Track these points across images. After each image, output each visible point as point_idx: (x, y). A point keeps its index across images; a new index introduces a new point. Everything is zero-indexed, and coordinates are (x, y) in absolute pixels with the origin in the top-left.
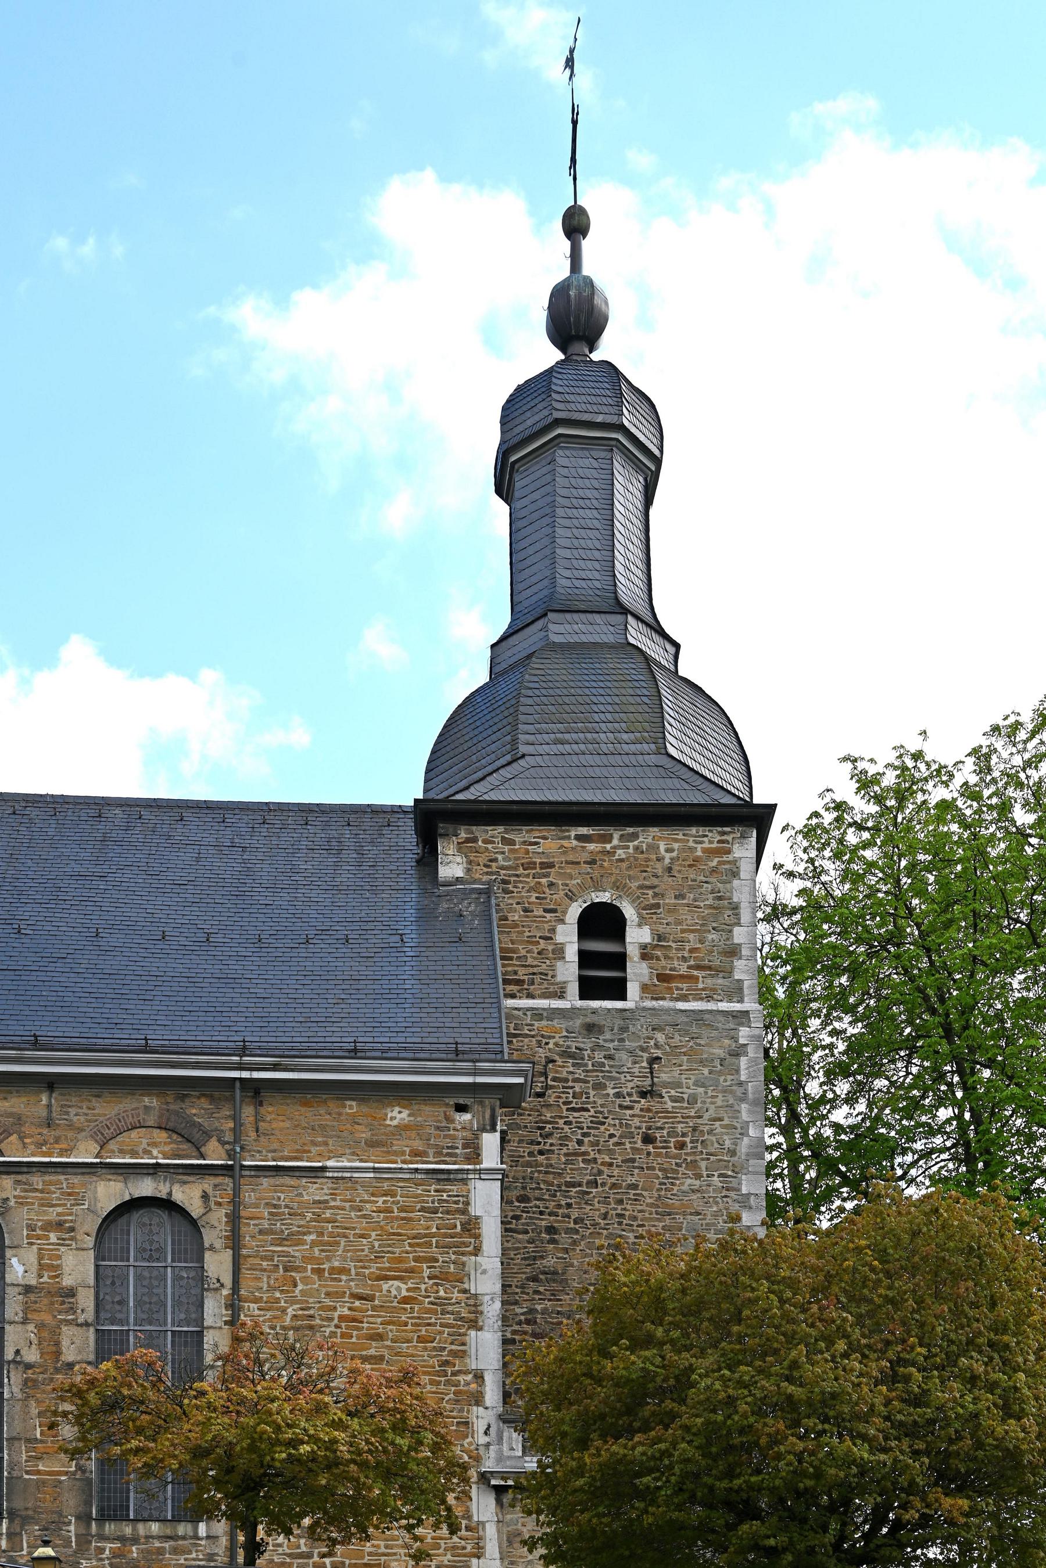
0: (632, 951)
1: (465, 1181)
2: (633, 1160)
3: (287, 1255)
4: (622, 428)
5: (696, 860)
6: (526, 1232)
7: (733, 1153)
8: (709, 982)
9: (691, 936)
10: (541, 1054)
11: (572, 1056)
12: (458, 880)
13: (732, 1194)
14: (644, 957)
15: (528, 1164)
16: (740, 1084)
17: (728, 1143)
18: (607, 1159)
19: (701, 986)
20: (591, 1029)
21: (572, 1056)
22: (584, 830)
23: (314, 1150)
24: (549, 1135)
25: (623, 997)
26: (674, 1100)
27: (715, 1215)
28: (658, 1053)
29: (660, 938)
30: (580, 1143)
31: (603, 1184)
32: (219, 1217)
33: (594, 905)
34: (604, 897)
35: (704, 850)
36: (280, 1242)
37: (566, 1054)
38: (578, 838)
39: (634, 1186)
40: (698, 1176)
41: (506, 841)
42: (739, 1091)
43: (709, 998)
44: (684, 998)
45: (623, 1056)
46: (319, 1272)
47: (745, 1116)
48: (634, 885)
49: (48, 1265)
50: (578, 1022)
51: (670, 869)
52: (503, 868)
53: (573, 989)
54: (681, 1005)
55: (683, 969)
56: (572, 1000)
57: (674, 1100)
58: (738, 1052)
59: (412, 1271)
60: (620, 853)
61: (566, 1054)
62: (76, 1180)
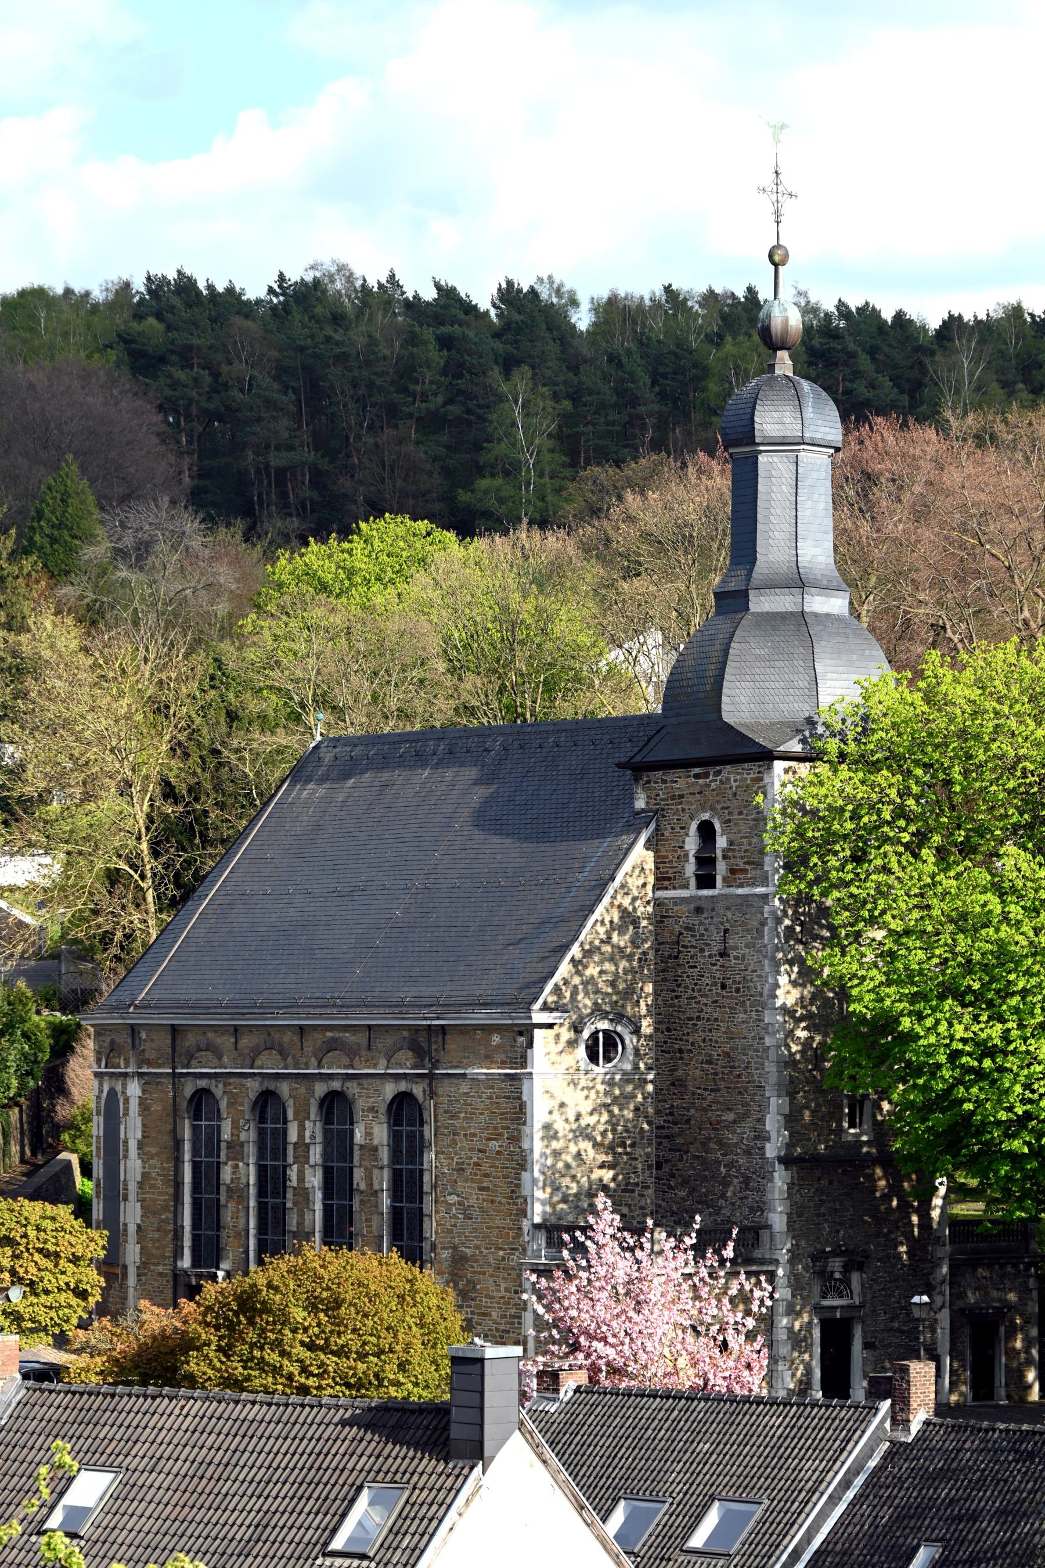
0: (719, 854)
1: (520, 1080)
3: (453, 1125)
5: (748, 786)
9: (745, 841)
10: (677, 928)
14: (725, 857)
20: (699, 910)
22: (697, 770)
23: (465, 1061)
24: (679, 986)
25: (714, 887)
28: (728, 925)
34: (706, 816)
37: (687, 929)
39: (716, 1020)
40: (745, 1012)
44: (741, 886)
45: (712, 928)
46: (465, 1135)
49: (369, 1134)
50: (692, 906)
53: (693, 882)
54: (740, 891)
55: (742, 866)
56: (692, 891)
57: (736, 958)
58: (763, 924)
59: (500, 1135)
61: (687, 929)
62: (378, 1082)
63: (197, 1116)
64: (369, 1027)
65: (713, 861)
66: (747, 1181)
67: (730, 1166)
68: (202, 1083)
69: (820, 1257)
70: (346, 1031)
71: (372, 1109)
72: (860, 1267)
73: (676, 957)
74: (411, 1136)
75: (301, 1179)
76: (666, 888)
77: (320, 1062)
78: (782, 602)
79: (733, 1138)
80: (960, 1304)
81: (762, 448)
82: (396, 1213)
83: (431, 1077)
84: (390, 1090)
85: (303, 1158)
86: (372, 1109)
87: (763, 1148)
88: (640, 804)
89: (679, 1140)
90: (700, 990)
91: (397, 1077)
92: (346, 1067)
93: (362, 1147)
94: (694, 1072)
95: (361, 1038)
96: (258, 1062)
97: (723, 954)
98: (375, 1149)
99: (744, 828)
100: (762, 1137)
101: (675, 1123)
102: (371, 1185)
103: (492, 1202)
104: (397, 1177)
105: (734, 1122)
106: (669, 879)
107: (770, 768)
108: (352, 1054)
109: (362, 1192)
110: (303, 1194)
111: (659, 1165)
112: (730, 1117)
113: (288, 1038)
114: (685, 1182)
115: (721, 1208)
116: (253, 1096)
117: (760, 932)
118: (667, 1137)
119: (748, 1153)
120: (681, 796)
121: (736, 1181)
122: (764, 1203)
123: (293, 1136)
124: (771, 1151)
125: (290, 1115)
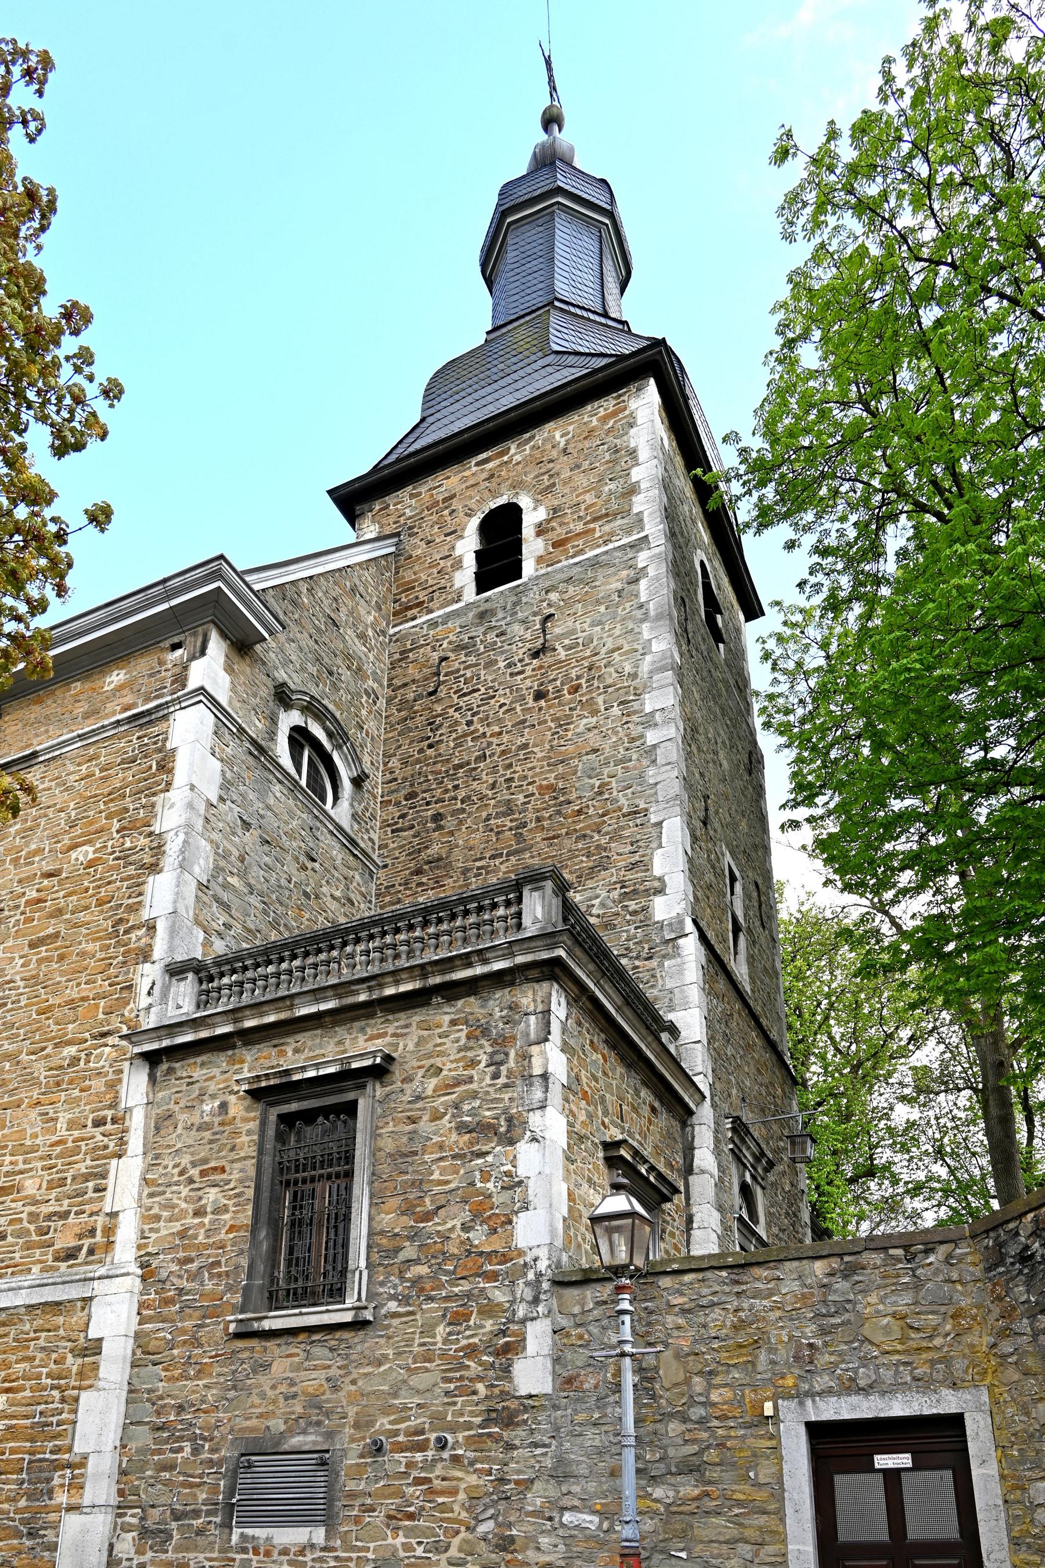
2: (524, 721)
4: (560, 191)
6: (412, 827)
7: (634, 676)
8: (607, 528)
10: (436, 656)
11: (463, 647)
13: (635, 718)
15: (418, 761)
17: (628, 668)
18: (497, 729)
19: (597, 535)
21: (463, 647)
27: (615, 747)
29: (555, 510)
30: (469, 723)
31: (492, 755)
33: (492, 511)
35: (599, 420)
37: (460, 647)
38: (477, 464)
39: (525, 746)
40: (595, 712)
42: (639, 614)
43: (605, 543)
48: (529, 478)
51: (565, 450)
52: (410, 518)
55: (579, 527)
57: (568, 648)
60: (518, 458)
61: (460, 647)
73: (431, 694)
76: (414, 618)
90: (481, 720)
106: (420, 604)
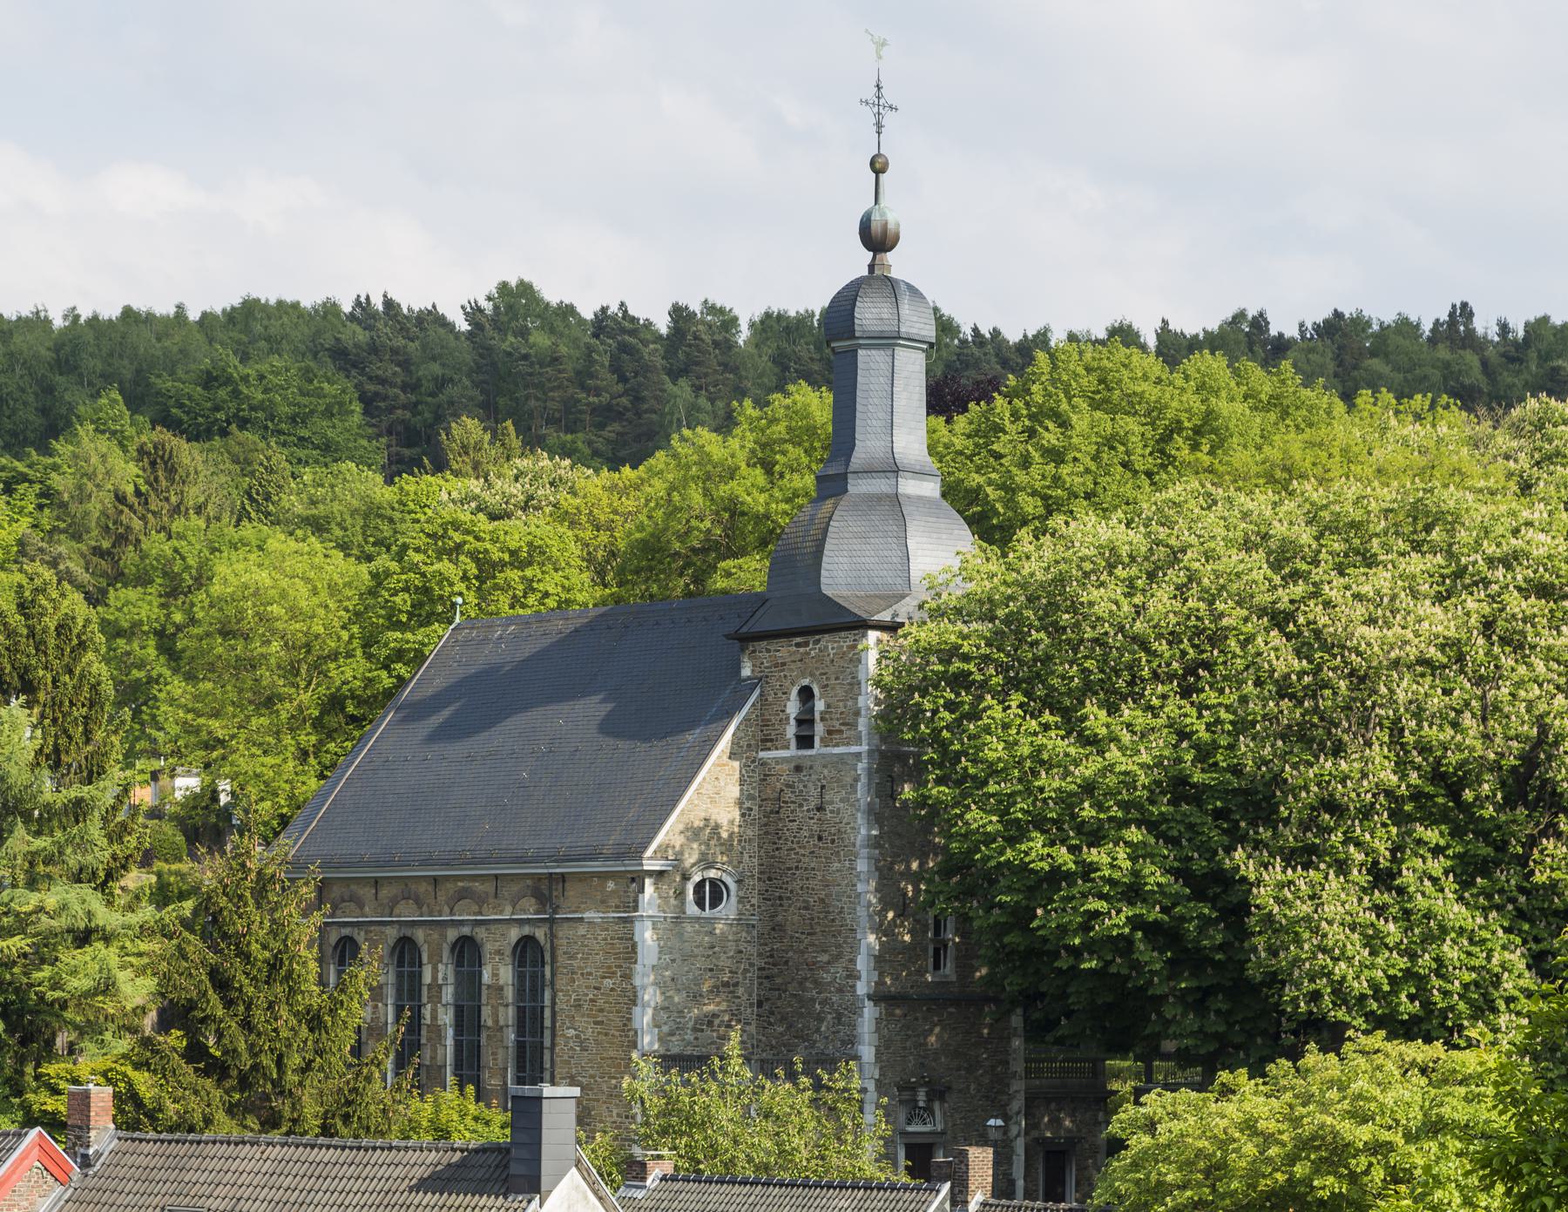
0: (817, 716)
1: (632, 922)
3: (571, 965)
5: (844, 653)
7: (854, 845)
9: (841, 704)
12: (749, 678)
14: (822, 719)
16: (858, 800)
22: (798, 640)
24: (779, 839)
26: (832, 812)
28: (824, 782)
32: (548, 945)
34: (806, 682)
36: (569, 958)
37: (788, 786)
39: (813, 869)
40: (840, 861)
41: (768, 651)
44: (837, 745)
46: (582, 974)
47: (860, 821)
49: (495, 975)
50: (793, 765)
53: (793, 743)
54: (837, 750)
55: (838, 727)
56: (792, 751)
57: (832, 812)
58: (857, 779)
61: (788, 786)
62: (505, 927)
63: (342, 962)
64: (496, 876)
65: (811, 722)
66: (839, 1016)
67: (824, 1002)
68: (346, 931)
69: (906, 1088)
70: (475, 881)
71: (499, 952)
72: (942, 1099)
74: (534, 977)
75: (434, 1017)
76: (769, 749)
77: (452, 910)
78: (880, 485)
79: (827, 977)
80: (1034, 1134)
81: (861, 342)
82: (520, 1046)
83: (551, 922)
84: (514, 934)
85: (436, 996)
86: (499, 952)
87: (854, 987)
88: (746, 671)
89: (778, 980)
90: (798, 842)
91: (521, 922)
92: (475, 914)
93: (489, 987)
94: (792, 917)
95: (489, 887)
96: (396, 911)
97: (820, 809)
98: (501, 988)
99: (840, 692)
100: (853, 975)
101: (774, 965)
102: (497, 1021)
103: (606, 1034)
104: (521, 1012)
105: (829, 963)
106: (772, 740)
107: (864, 636)
108: (481, 901)
109: (489, 1028)
110: (437, 1031)
111: (760, 1004)
112: (825, 958)
113: (423, 888)
114: (783, 1019)
115: (815, 1042)
116: (391, 942)
117: (853, 787)
118: (767, 977)
119: (840, 990)
120: (784, 664)
121: (829, 1016)
122: (855, 1037)
123: (427, 978)
124: (862, 988)
125: (425, 959)
